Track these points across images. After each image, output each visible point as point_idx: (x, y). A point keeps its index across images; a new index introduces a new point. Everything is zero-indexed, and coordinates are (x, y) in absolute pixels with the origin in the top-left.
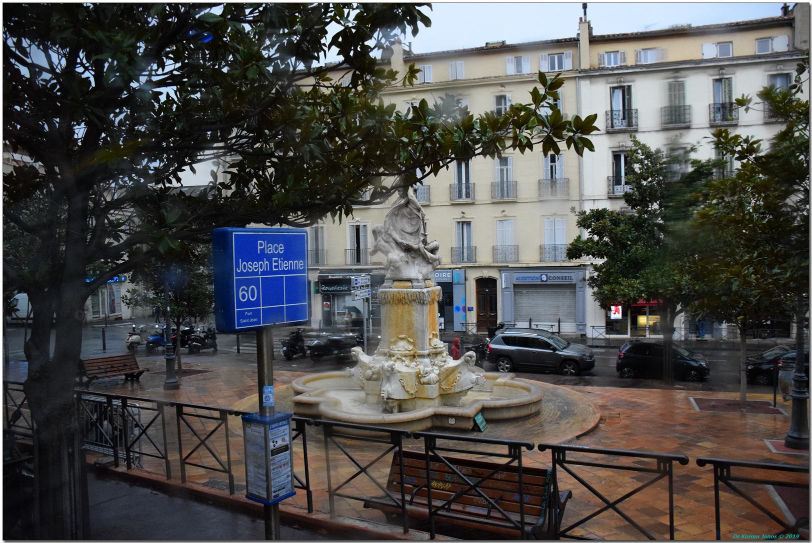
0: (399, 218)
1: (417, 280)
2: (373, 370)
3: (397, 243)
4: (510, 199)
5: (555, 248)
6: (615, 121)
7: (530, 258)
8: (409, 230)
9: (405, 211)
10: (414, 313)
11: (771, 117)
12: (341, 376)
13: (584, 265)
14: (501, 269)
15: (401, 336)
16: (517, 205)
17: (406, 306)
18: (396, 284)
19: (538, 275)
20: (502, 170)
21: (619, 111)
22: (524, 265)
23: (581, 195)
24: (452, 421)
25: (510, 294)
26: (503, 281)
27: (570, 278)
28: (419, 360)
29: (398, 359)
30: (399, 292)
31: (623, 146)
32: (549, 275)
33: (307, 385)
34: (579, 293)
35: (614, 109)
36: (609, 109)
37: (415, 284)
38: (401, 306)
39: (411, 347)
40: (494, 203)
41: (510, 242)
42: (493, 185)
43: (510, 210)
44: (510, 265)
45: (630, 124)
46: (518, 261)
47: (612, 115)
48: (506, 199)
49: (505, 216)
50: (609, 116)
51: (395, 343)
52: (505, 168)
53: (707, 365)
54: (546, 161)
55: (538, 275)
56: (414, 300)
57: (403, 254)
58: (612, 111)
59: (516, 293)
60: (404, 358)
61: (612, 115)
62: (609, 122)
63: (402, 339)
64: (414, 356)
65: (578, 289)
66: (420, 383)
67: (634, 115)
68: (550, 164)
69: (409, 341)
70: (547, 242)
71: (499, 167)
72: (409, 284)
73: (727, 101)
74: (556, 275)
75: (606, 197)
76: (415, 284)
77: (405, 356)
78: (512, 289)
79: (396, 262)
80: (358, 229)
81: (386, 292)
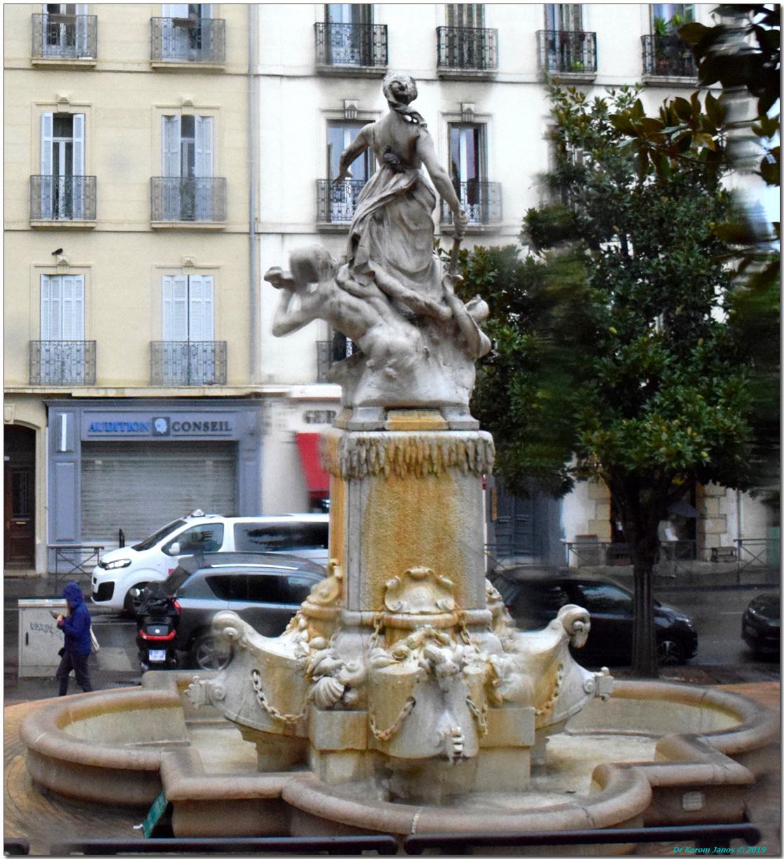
0: (385, 229)
1: (458, 406)
2: (345, 676)
3: (390, 296)
4: (77, 222)
5: (188, 349)
6: (335, 50)
7: (121, 372)
8: (410, 264)
9: (402, 209)
10: (454, 501)
11: (658, 71)
12: (130, 706)
13: (258, 395)
14: (48, 402)
15: (414, 571)
16: (93, 236)
17: (431, 482)
18: (393, 417)
19: (144, 418)
20: (56, 146)
21: (341, 24)
22: (112, 393)
23: (253, 220)
24: (694, 803)
25: (70, 469)
26: (58, 436)
27: (224, 426)
28: (472, 637)
29: (429, 637)
30: (412, 442)
31: (352, 108)
32: (175, 418)
33: (69, 730)
34: (244, 465)
35: (335, 18)
36: (322, 19)
37: (454, 417)
38: (413, 483)
39: (451, 603)
40: (35, 229)
41: (72, 332)
42: (34, 183)
43: (75, 250)
44: (76, 393)
45: (368, 58)
46: (93, 382)
47: (328, 33)
48: (63, 220)
49: (64, 264)
50: (322, 37)
51: (398, 590)
52: (63, 141)
53: (694, 623)
54: (169, 133)
55: (144, 418)
56: (457, 465)
57: (415, 333)
58: (327, 23)
59: (86, 465)
60: (445, 636)
61: (328, 33)
62: (322, 48)
63: (417, 579)
64: (458, 629)
65: (243, 455)
66: (492, 703)
67: (378, 38)
68: (179, 139)
69: (439, 585)
70: (169, 333)
71: (51, 139)
72: (436, 418)
73: (572, 27)
74: (191, 418)
75: (311, 229)
76: (454, 417)
77: (444, 629)
78: (78, 456)
79: (404, 353)
80: (36, 267)
81: (373, 442)
